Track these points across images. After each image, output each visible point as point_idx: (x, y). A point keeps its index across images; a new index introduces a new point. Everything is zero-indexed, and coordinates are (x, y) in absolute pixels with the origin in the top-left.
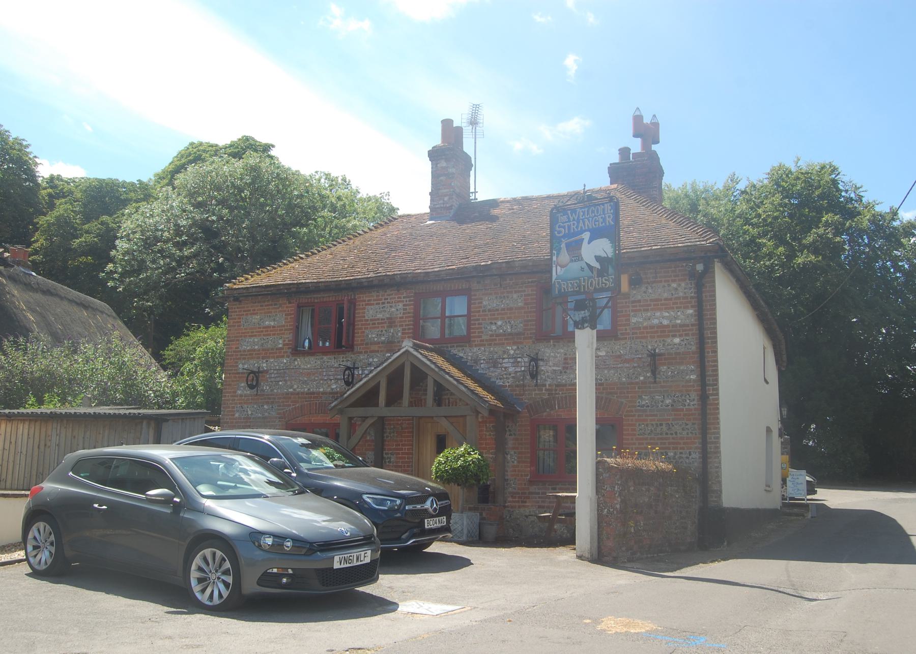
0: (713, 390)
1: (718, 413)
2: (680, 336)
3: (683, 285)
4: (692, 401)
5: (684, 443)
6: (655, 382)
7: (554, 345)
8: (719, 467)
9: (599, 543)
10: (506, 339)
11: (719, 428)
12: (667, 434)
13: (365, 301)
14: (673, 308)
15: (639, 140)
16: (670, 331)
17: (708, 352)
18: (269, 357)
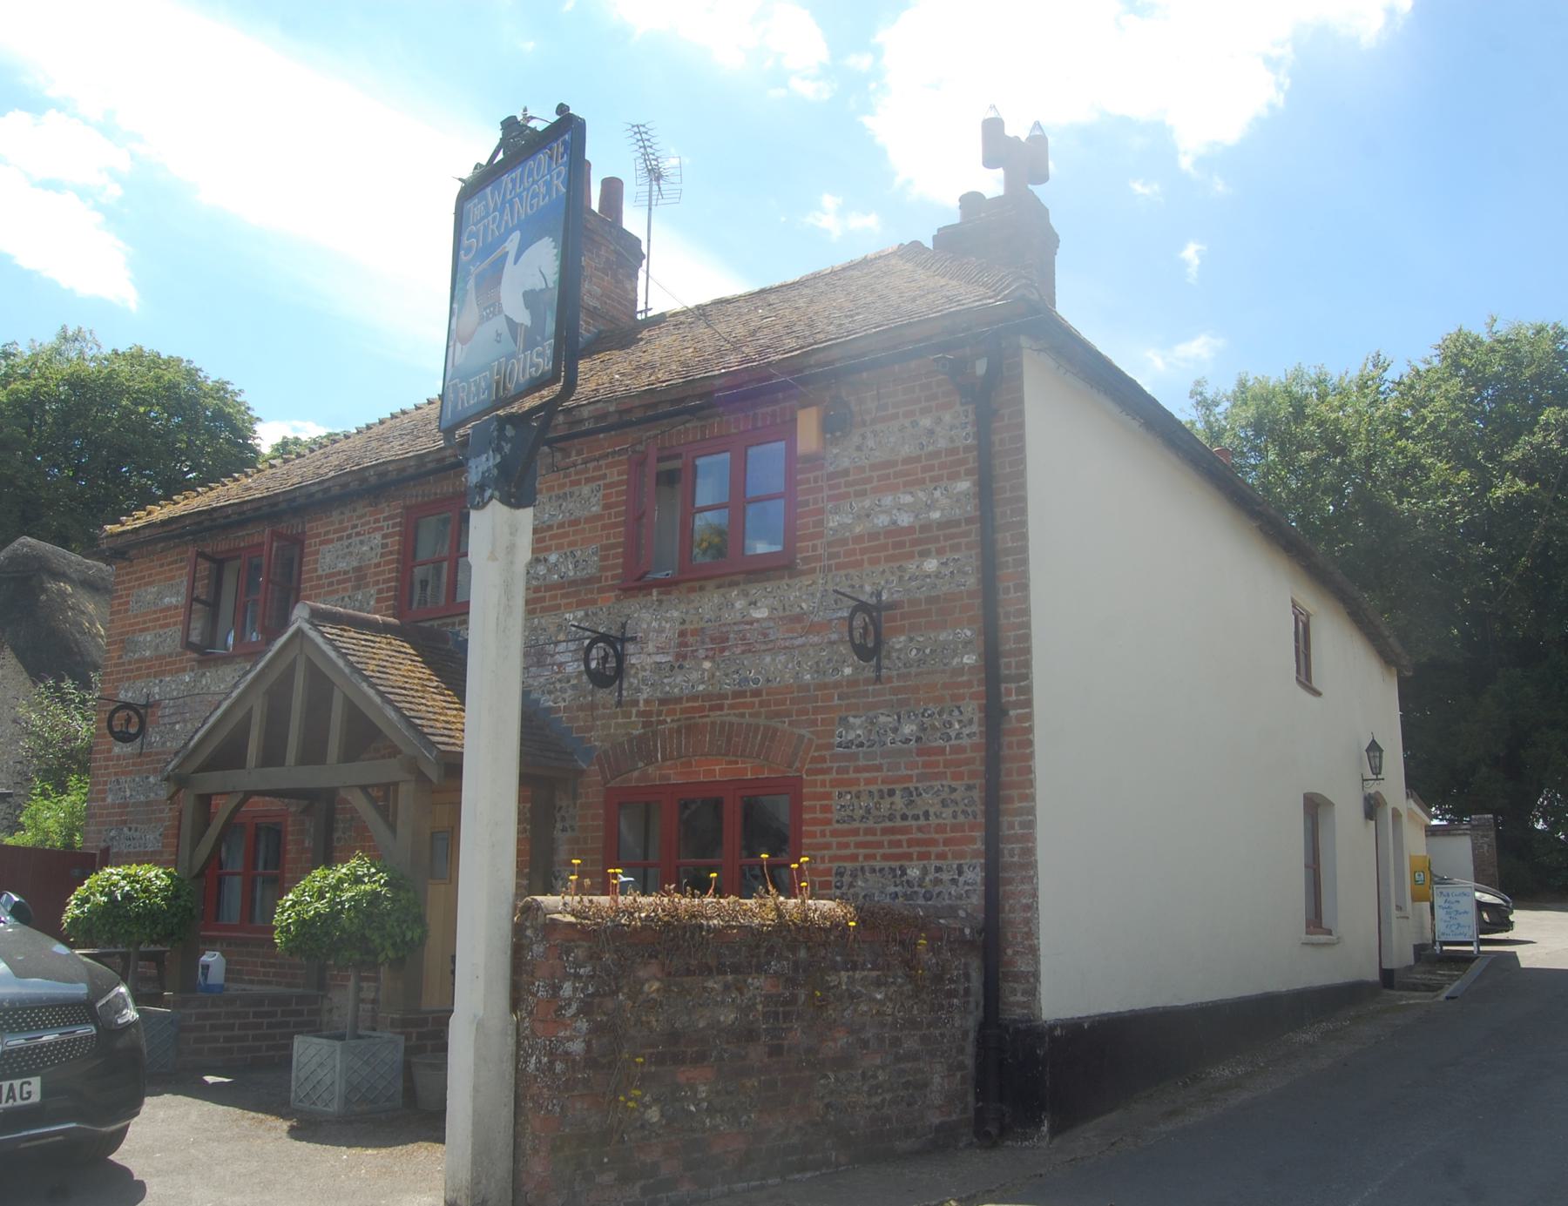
0: (1020, 691)
1: (1031, 756)
2: (940, 552)
3: (947, 418)
4: (966, 727)
5: (946, 842)
6: (878, 679)
7: (660, 602)
8: (1031, 908)
9: (515, 1160)
10: (564, 596)
11: (1032, 798)
12: (904, 817)
13: (318, 535)
14: (923, 481)
15: (999, 173)
16: (915, 543)
17: (1007, 590)
18: (163, 673)
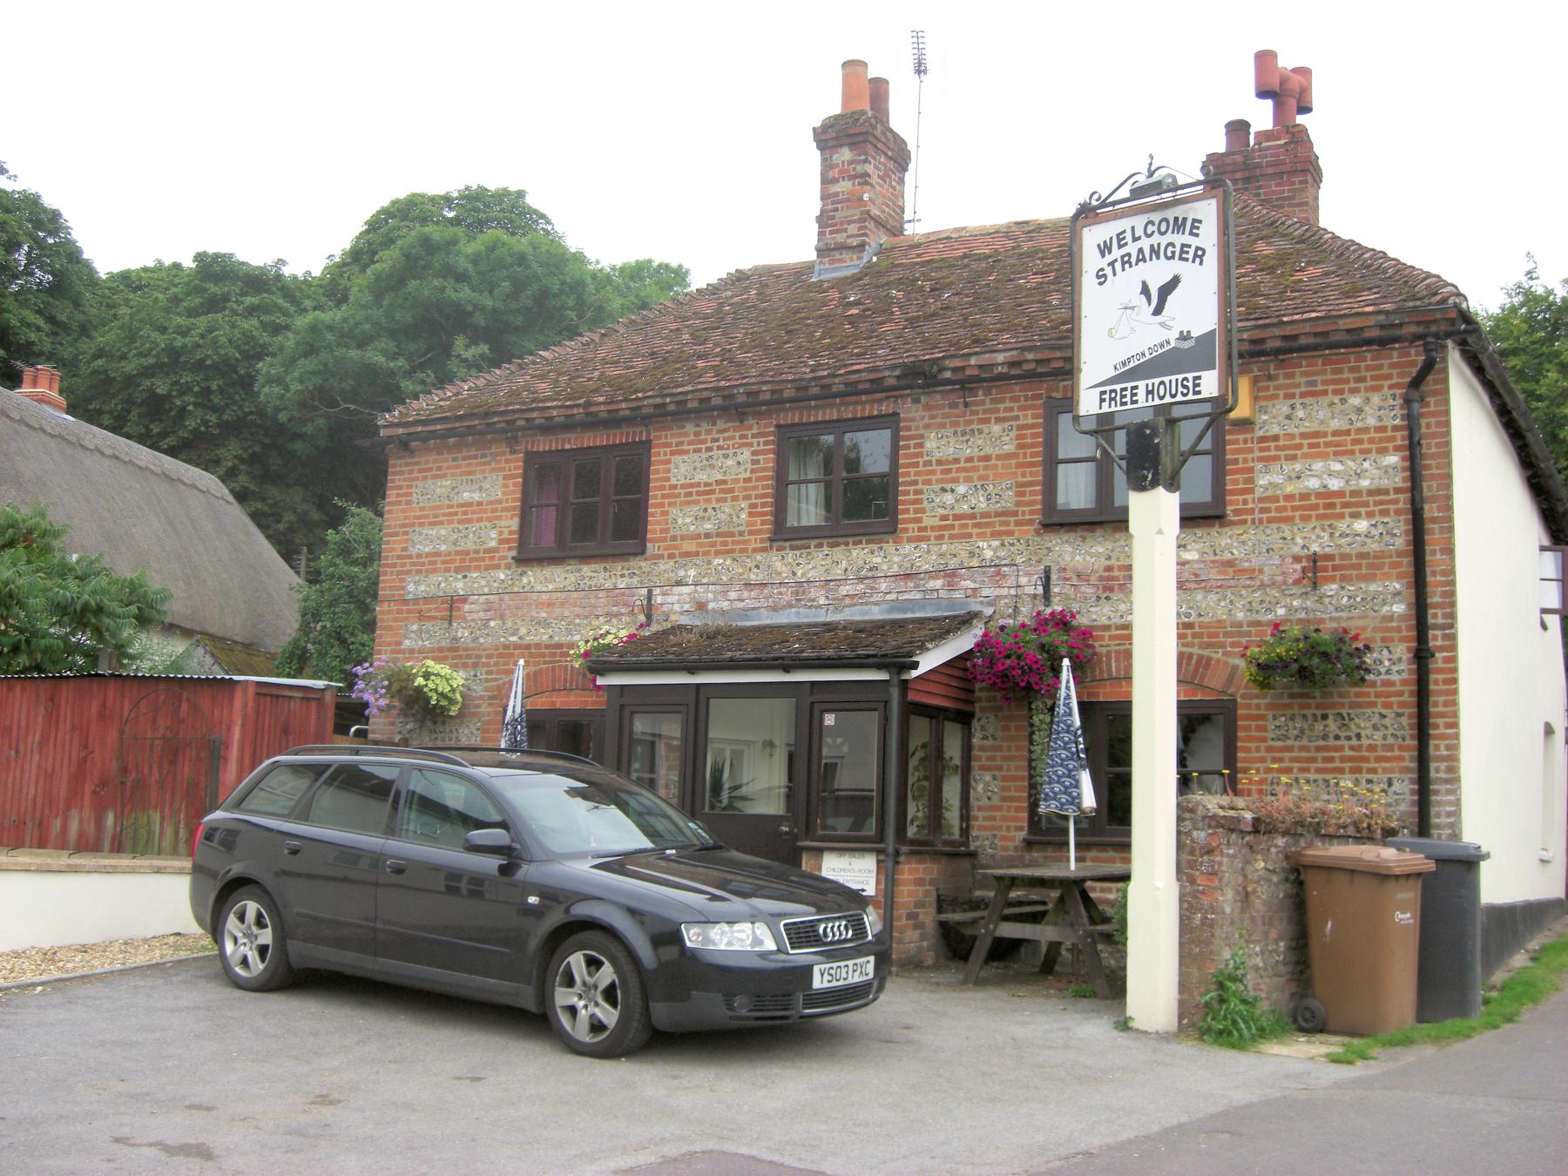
2: (1370, 515)
12: (1337, 737)
14: (1352, 452)
15: (1268, 104)
16: (1346, 505)
18: (468, 569)
